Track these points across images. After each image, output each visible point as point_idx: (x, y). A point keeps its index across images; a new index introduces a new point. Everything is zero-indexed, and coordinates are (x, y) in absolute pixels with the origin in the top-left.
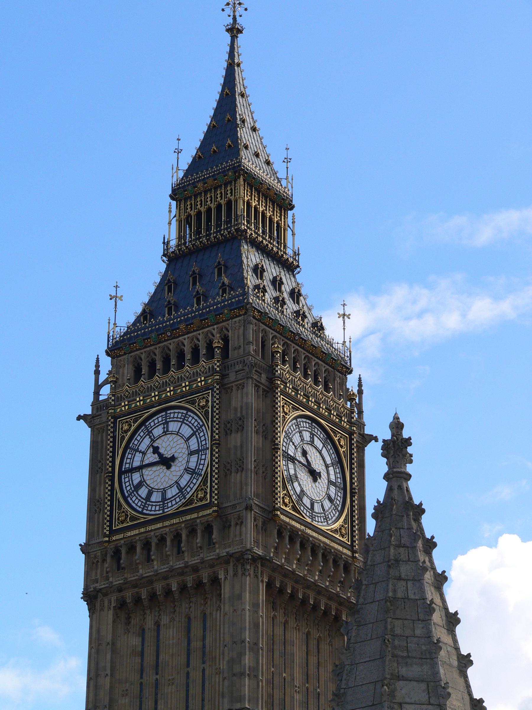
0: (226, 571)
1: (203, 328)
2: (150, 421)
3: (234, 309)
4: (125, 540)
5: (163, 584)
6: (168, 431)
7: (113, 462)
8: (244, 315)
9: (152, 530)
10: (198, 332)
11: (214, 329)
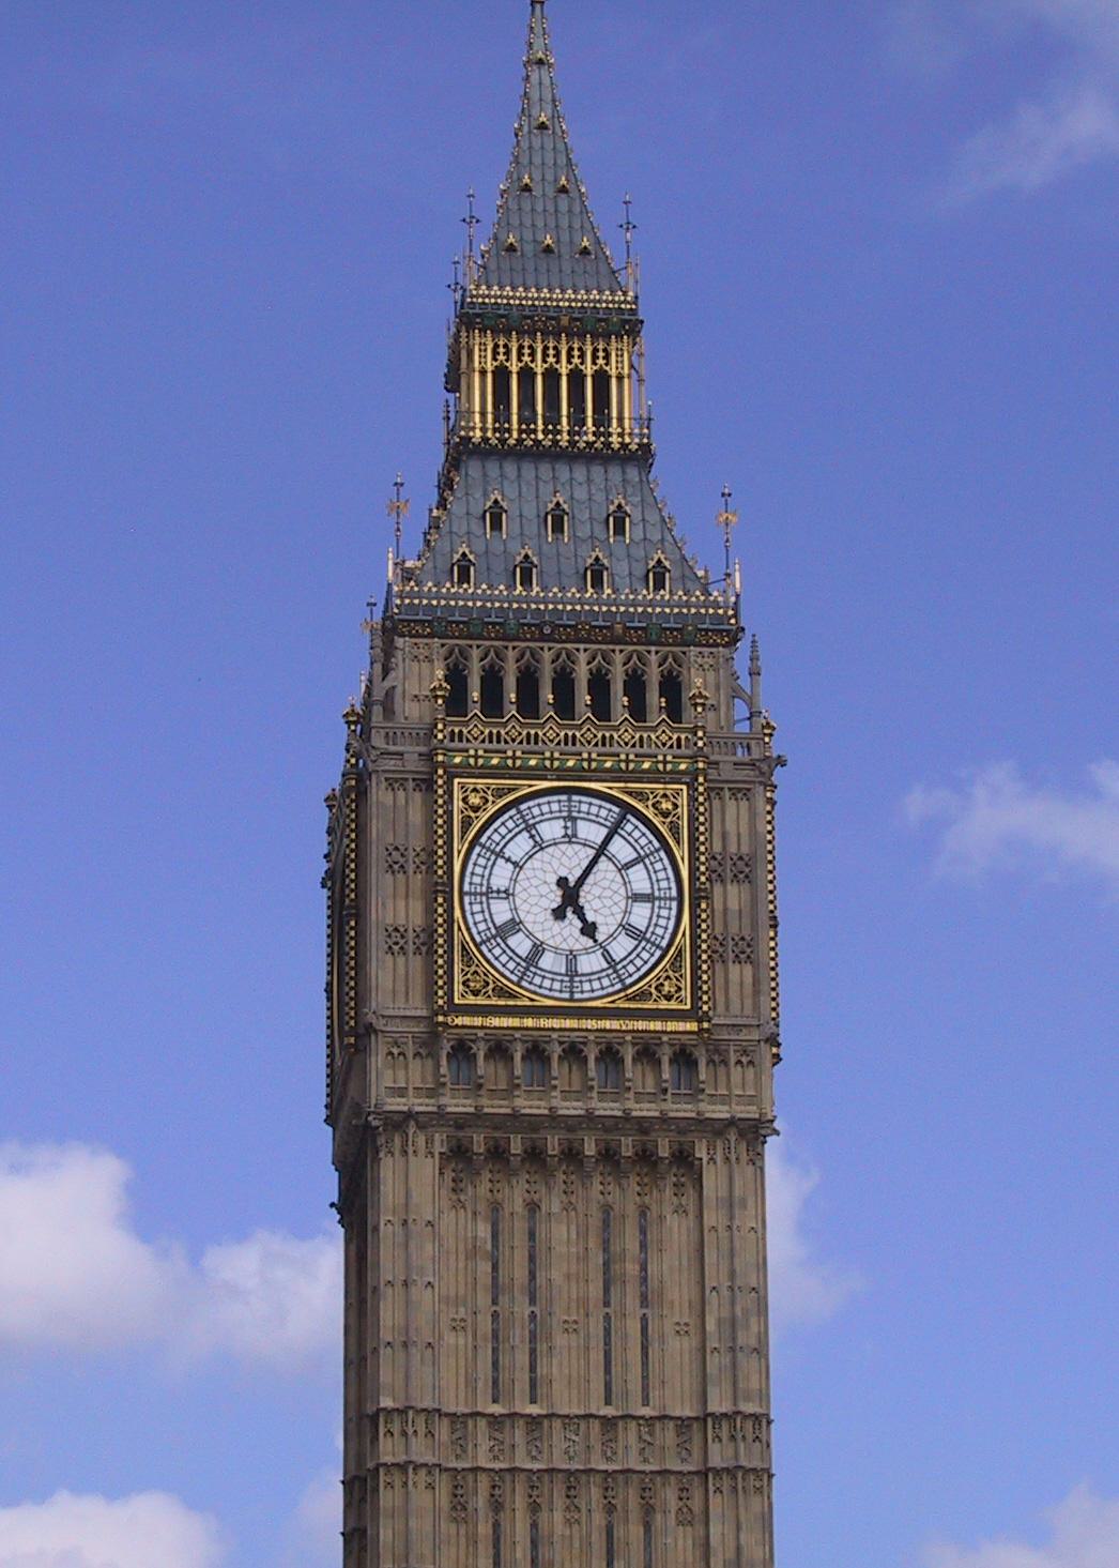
0: (711, 1147)
1: (626, 643)
2: (531, 803)
3: (707, 630)
4: (488, 1031)
5: (561, 1137)
6: (575, 836)
7: (450, 863)
8: (724, 646)
9: (553, 1029)
10: (611, 647)
11: (649, 652)
